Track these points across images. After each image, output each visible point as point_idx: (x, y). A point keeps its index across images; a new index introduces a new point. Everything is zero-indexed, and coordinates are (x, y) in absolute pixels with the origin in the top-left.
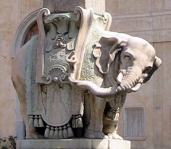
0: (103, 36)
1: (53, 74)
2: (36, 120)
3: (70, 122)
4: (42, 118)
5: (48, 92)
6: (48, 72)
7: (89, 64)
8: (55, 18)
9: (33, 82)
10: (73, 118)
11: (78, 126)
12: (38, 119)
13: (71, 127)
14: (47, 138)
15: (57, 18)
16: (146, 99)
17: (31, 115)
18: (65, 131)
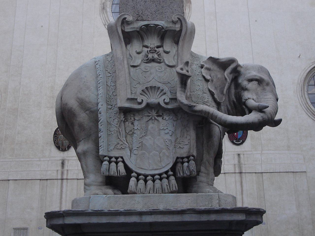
0: (212, 56)
2: (113, 164)
3: (173, 169)
4: (123, 162)
5: (136, 123)
6: (139, 91)
7: (199, 87)
8: (143, 26)
9: (110, 107)
10: (179, 161)
11: (188, 174)
12: (117, 163)
13: (174, 175)
14: (135, 193)
15: (147, 26)
16: (31, 221)
17: (105, 156)
18: (165, 181)
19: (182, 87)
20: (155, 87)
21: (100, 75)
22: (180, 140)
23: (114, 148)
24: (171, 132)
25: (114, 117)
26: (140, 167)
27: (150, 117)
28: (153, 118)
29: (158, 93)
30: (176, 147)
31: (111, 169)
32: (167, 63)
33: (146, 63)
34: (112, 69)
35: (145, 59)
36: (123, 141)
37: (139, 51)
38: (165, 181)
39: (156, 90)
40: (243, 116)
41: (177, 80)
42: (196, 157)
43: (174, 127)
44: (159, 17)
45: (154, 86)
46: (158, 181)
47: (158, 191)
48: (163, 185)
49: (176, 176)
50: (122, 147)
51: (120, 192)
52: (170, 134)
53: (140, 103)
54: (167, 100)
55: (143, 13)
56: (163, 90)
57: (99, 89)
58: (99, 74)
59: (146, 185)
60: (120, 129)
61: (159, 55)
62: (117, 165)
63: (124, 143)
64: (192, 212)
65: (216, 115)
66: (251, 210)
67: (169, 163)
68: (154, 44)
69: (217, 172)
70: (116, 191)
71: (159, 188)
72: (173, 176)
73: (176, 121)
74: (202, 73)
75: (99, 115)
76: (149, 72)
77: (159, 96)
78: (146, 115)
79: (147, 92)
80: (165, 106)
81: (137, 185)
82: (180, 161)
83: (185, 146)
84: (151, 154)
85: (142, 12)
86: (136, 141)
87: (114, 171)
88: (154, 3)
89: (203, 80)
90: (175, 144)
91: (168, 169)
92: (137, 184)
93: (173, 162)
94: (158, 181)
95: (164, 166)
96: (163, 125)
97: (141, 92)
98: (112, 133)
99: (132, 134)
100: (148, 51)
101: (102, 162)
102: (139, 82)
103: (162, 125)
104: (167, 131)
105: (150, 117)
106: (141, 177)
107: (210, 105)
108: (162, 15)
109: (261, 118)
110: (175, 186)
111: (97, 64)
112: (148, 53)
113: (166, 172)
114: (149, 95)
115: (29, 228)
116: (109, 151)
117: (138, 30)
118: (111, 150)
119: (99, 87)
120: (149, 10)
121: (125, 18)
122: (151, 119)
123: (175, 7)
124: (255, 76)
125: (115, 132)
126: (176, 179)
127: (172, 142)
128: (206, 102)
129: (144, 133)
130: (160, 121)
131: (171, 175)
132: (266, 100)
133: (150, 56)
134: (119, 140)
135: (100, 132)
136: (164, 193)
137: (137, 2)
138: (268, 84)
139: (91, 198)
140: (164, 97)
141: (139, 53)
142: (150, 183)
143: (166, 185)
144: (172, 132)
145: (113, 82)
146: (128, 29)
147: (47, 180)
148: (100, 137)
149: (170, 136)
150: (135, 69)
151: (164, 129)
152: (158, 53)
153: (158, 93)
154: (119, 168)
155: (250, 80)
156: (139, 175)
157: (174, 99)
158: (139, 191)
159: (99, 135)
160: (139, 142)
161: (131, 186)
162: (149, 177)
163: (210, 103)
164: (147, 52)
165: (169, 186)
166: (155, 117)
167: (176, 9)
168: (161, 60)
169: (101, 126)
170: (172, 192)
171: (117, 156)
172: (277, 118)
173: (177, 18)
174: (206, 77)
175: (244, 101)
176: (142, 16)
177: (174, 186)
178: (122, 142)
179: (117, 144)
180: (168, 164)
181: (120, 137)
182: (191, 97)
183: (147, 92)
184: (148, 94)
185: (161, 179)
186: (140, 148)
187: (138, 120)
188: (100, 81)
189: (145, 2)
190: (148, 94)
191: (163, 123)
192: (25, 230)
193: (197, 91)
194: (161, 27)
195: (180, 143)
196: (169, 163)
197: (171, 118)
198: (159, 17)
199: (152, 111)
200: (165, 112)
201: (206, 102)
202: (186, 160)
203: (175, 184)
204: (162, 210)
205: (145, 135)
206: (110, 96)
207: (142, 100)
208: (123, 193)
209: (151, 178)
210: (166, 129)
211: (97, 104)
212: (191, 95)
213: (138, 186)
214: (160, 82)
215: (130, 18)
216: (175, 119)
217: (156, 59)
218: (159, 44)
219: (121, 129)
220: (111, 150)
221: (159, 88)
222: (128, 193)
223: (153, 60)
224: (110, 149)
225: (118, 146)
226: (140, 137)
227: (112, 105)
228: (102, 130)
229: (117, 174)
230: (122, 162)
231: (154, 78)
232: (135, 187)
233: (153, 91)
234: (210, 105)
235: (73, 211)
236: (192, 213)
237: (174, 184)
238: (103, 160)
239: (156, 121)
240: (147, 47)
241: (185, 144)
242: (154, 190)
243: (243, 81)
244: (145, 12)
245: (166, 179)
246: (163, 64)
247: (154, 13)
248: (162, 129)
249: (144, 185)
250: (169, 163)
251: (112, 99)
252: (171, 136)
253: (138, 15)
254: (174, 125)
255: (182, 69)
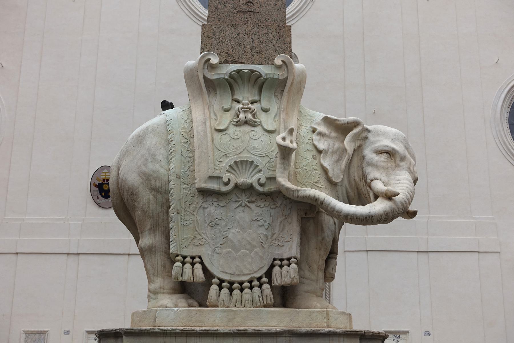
1: (235, 171)
2: (188, 266)
3: (269, 274)
4: (202, 263)
12: (193, 264)
13: (270, 283)
14: (216, 306)
15: (238, 71)
17: (178, 255)
18: (256, 290)
19: (283, 163)
20: (247, 161)
21: (172, 141)
22: (279, 234)
23: (189, 243)
24: (266, 224)
25: (191, 202)
26: (223, 271)
27: (240, 203)
28: (243, 205)
29: (252, 169)
30: (273, 244)
31: (185, 272)
32: (266, 127)
33: (236, 126)
34: (189, 133)
35: (235, 120)
36: (202, 235)
37: (227, 108)
38: (256, 290)
39: (248, 166)
40: (364, 205)
41: (276, 152)
42: (298, 261)
43: (272, 217)
44: (256, 57)
45: (245, 160)
46: (247, 291)
47: (246, 305)
48: (254, 297)
49: (272, 284)
50: (200, 243)
51: (196, 303)
52: (266, 227)
53: (227, 184)
54: (263, 181)
55: (234, 51)
56: (258, 166)
57: (170, 161)
58: (171, 140)
59: (231, 296)
60: (198, 218)
61: (254, 116)
62: (193, 267)
63: (203, 238)
64: (291, 334)
65: (327, 202)
66: (368, 334)
67: (263, 267)
68: (248, 97)
69: (329, 277)
70: (191, 301)
71: (248, 299)
72: (267, 284)
73: (275, 209)
74: (313, 141)
75: (171, 198)
76: (240, 140)
77: (251, 176)
78: (234, 200)
79: (235, 168)
80: (260, 189)
81: (219, 295)
82: (278, 264)
83: (285, 243)
84: (239, 253)
85: (232, 49)
86: (220, 235)
87: (189, 276)
88: (251, 37)
89: (314, 150)
90: (273, 241)
91: (262, 274)
92: (220, 293)
93: (268, 264)
94: (247, 291)
95: (256, 270)
96: (256, 214)
97: (228, 168)
98: (187, 224)
99: (214, 225)
100: (239, 109)
101: (173, 262)
102: (225, 154)
103: (255, 214)
104: (260, 223)
105: (240, 203)
106: (224, 284)
107: (321, 187)
108: (261, 54)
109: (388, 209)
110: (270, 298)
111: (168, 125)
112: (240, 112)
113: (259, 279)
114: (238, 172)
115: (49, 331)
116: (183, 248)
117: (227, 78)
118: (186, 246)
119: (171, 159)
120: (242, 47)
121: (209, 60)
122: (241, 205)
123: (279, 43)
124: (387, 146)
125: (192, 222)
126: (272, 288)
127: (268, 238)
128: (316, 183)
129: (231, 224)
130: (253, 209)
131: (265, 283)
132: (399, 182)
133: (242, 116)
134: (197, 232)
135: (171, 221)
136: (255, 307)
137: (227, 34)
138: (403, 159)
139: (158, 312)
140: (258, 176)
141: (227, 111)
142: (236, 292)
143: (258, 295)
144: (269, 224)
145: (190, 151)
146: (213, 76)
147: (79, 254)
148: (172, 229)
149: (265, 230)
150: (220, 134)
151: (258, 220)
152: (253, 111)
153: (252, 169)
154: (195, 271)
155: (379, 152)
156: (222, 281)
157: (272, 179)
158: (221, 303)
159: (171, 226)
160: (224, 237)
161: (211, 297)
162: (236, 285)
163: (322, 184)
164: (237, 109)
165: (262, 298)
166: (246, 202)
167: (281, 46)
168: (256, 123)
169: (173, 214)
170: (265, 306)
171: (194, 255)
172: (411, 208)
173: (282, 61)
174: (318, 147)
175: (369, 181)
176: (233, 55)
177: (269, 298)
178: (201, 236)
179: (193, 239)
180: (262, 267)
181: (197, 229)
182: (296, 175)
183: (235, 168)
184: (238, 171)
185: (251, 288)
186: (225, 245)
187: (223, 207)
188: (173, 150)
189: (237, 35)
190: (238, 172)
191: (256, 212)
192: (43, 335)
193: (305, 166)
194: (258, 73)
195: (278, 239)
196: (263, 267)
197: (267, 205)
198: (256, 57)
199: (241, 195)
200: (259, 196)
201: (316, 183)
202: (285, 262)
203: (270, 296)
204: (250, 331)
205: (231, 227)
206: (186, 172)
207: (229, 179)
208: (201, 305)
209: (238, 287)
210: (261, 219)
211: (168, 182)
212: (297, 173)
213: (220, 296)
214: (254, 155)
215: (215, 60)
216: (273, 206)
217: (250, 121)
218: (256, 98)
219: (199, 218)
220: (186, 246)
221: (252, 163)
222: (207, 307)
223: (246, 122)
224: (184, 245)
225: (196, 241)
226: (226, 230)
227: (188, 184)
228: (173, 219)
229: (193, 280)
230: (200, 263)
231: (245, 148)
232: (216, 297)
233: (244, 166)
234: (322, 187)
235: (135, 330)
236: (289, 336)
237: (269, 296)
238: (175, 260)
239: (248, 208)
240: (238, 102)
241: (285, 241)
242: (242, 303)
243: (369, 154)
244: (237, 50)
245: (258, 287)
246: (260, 127)
247: (250, 51)
248: (254, 219)
249: (229, 295)
250: (262, 266)
251: (188, 175)
252: (266, 229)
253: (227, 53)
254: (271, 215)
255: (284, 139)
